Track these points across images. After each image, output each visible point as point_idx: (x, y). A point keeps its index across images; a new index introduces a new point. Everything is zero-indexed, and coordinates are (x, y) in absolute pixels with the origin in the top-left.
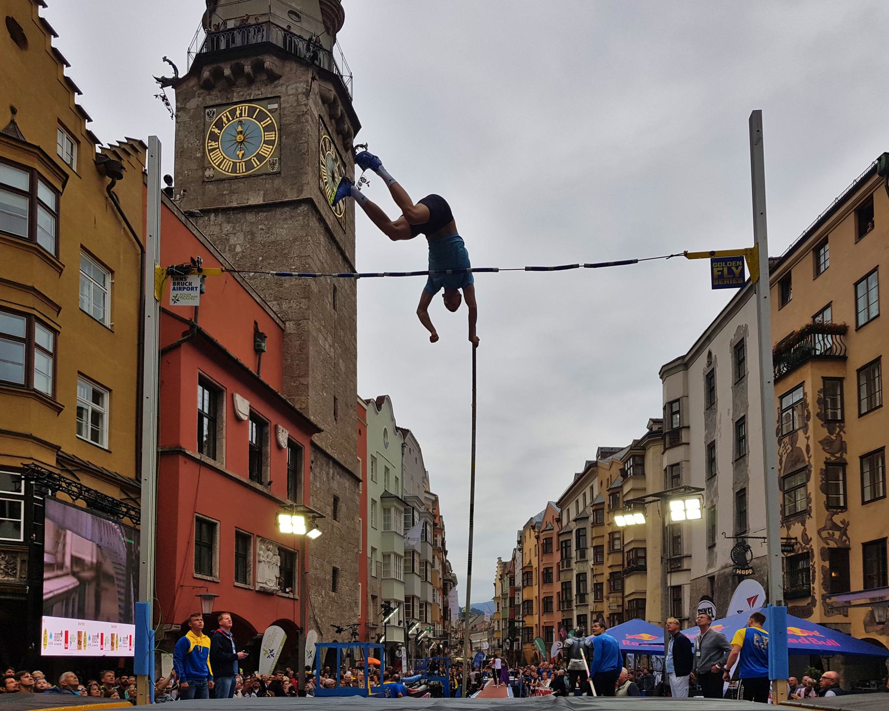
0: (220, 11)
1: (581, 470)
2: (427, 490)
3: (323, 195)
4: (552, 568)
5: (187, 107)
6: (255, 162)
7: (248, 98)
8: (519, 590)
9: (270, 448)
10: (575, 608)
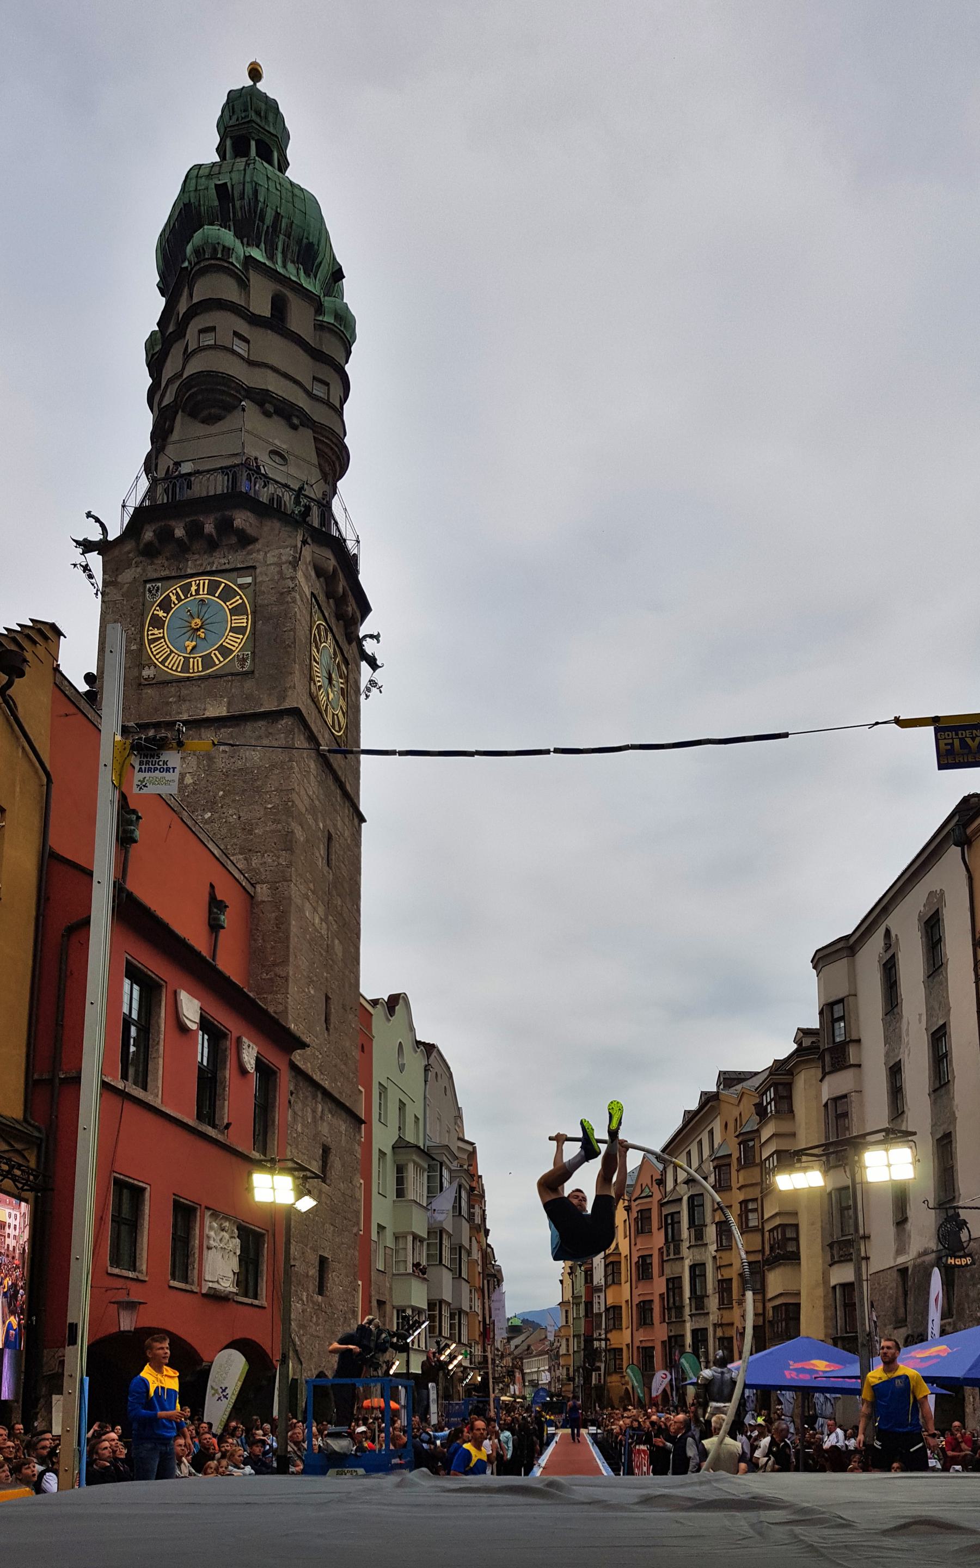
0: (170, 450)
1: (694, 1105)
2: (461, 1136)
3: (315, 704)
4: (651, 1255)
5: (119, 580)
6: (217, 658)
7: (208, 569)
8: (599, 1289)
9: (229, 1073)
10: (687, 1318)
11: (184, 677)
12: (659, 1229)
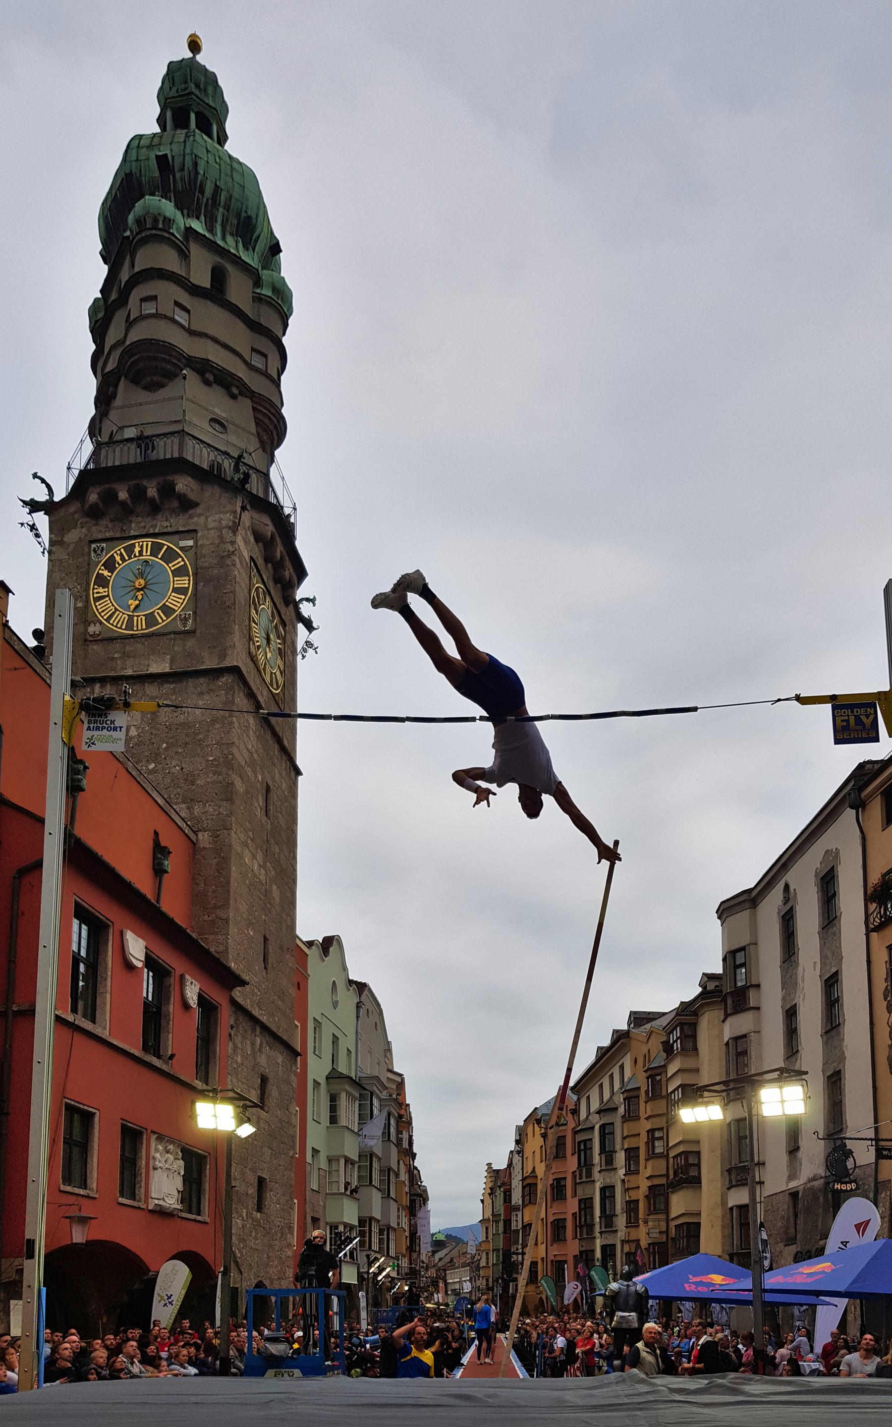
2: (390, 1067)
4: (565, 1178)
5: (65, 539)
6: (160, 616)
7: (152, 531)
8: (516, 1209)
9: (173, 1008)
11: (128, 635)
12: (572, 1155)
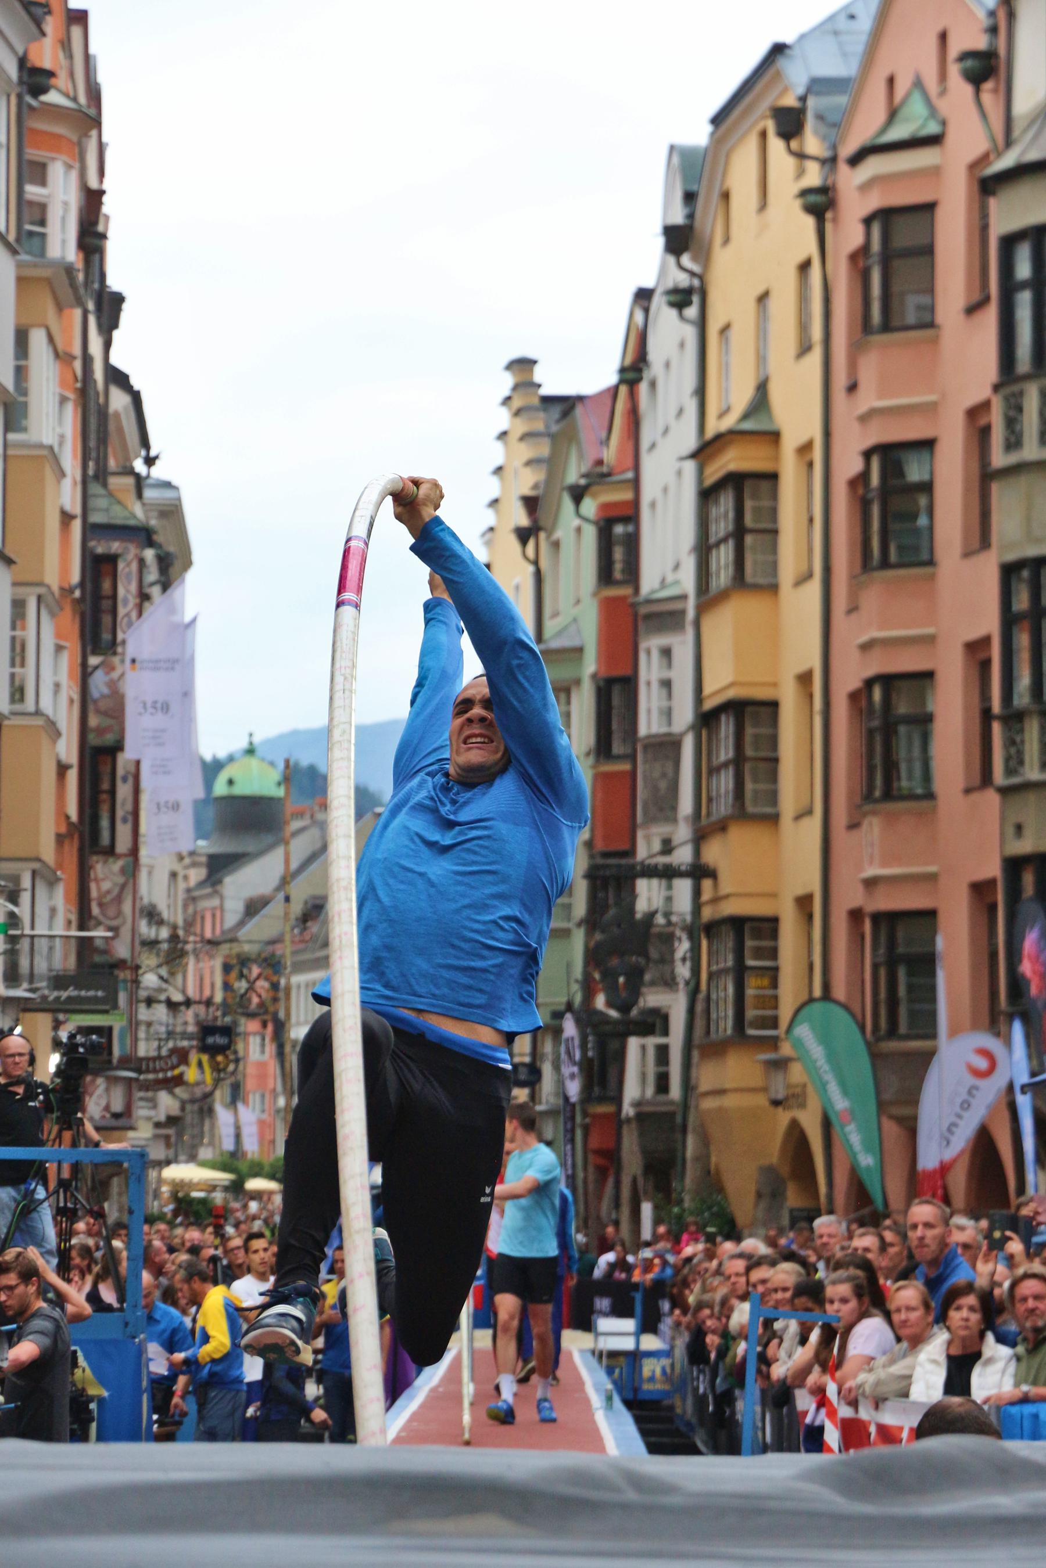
4: (928, 445)
12: (972, 309)
